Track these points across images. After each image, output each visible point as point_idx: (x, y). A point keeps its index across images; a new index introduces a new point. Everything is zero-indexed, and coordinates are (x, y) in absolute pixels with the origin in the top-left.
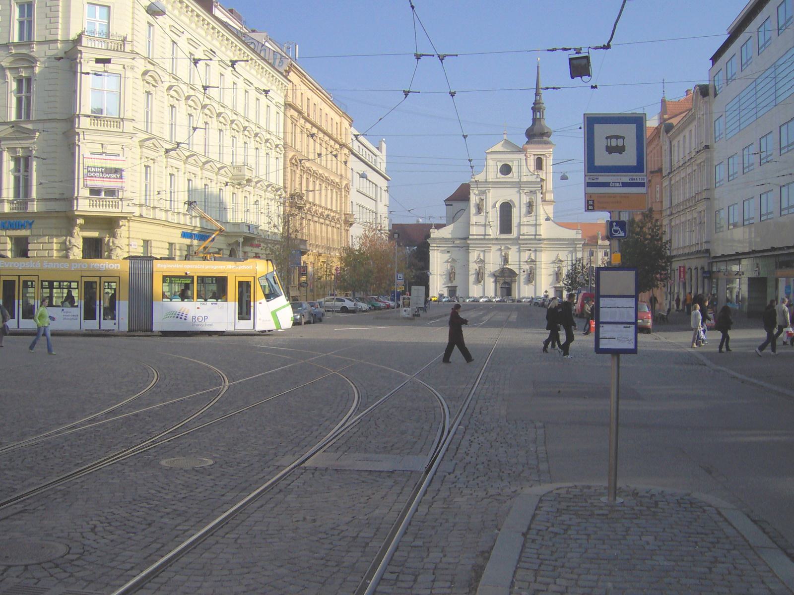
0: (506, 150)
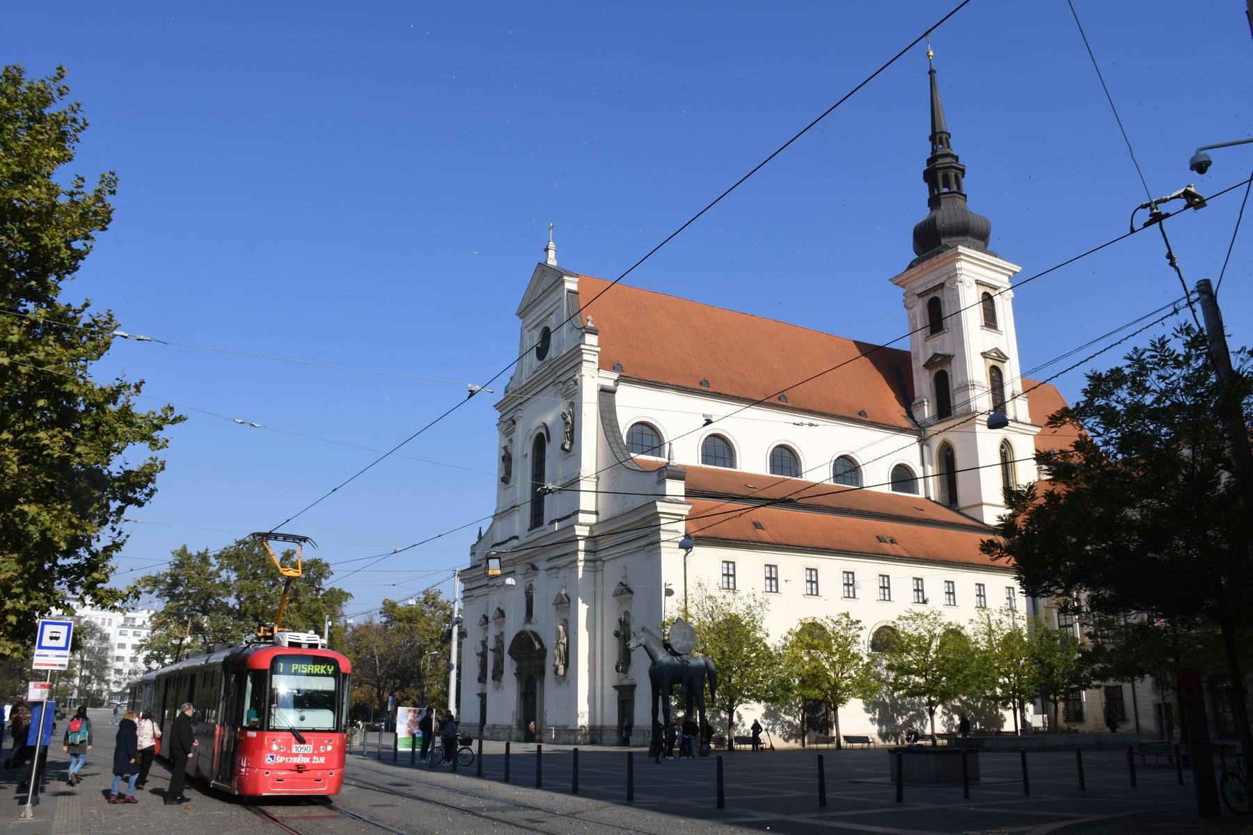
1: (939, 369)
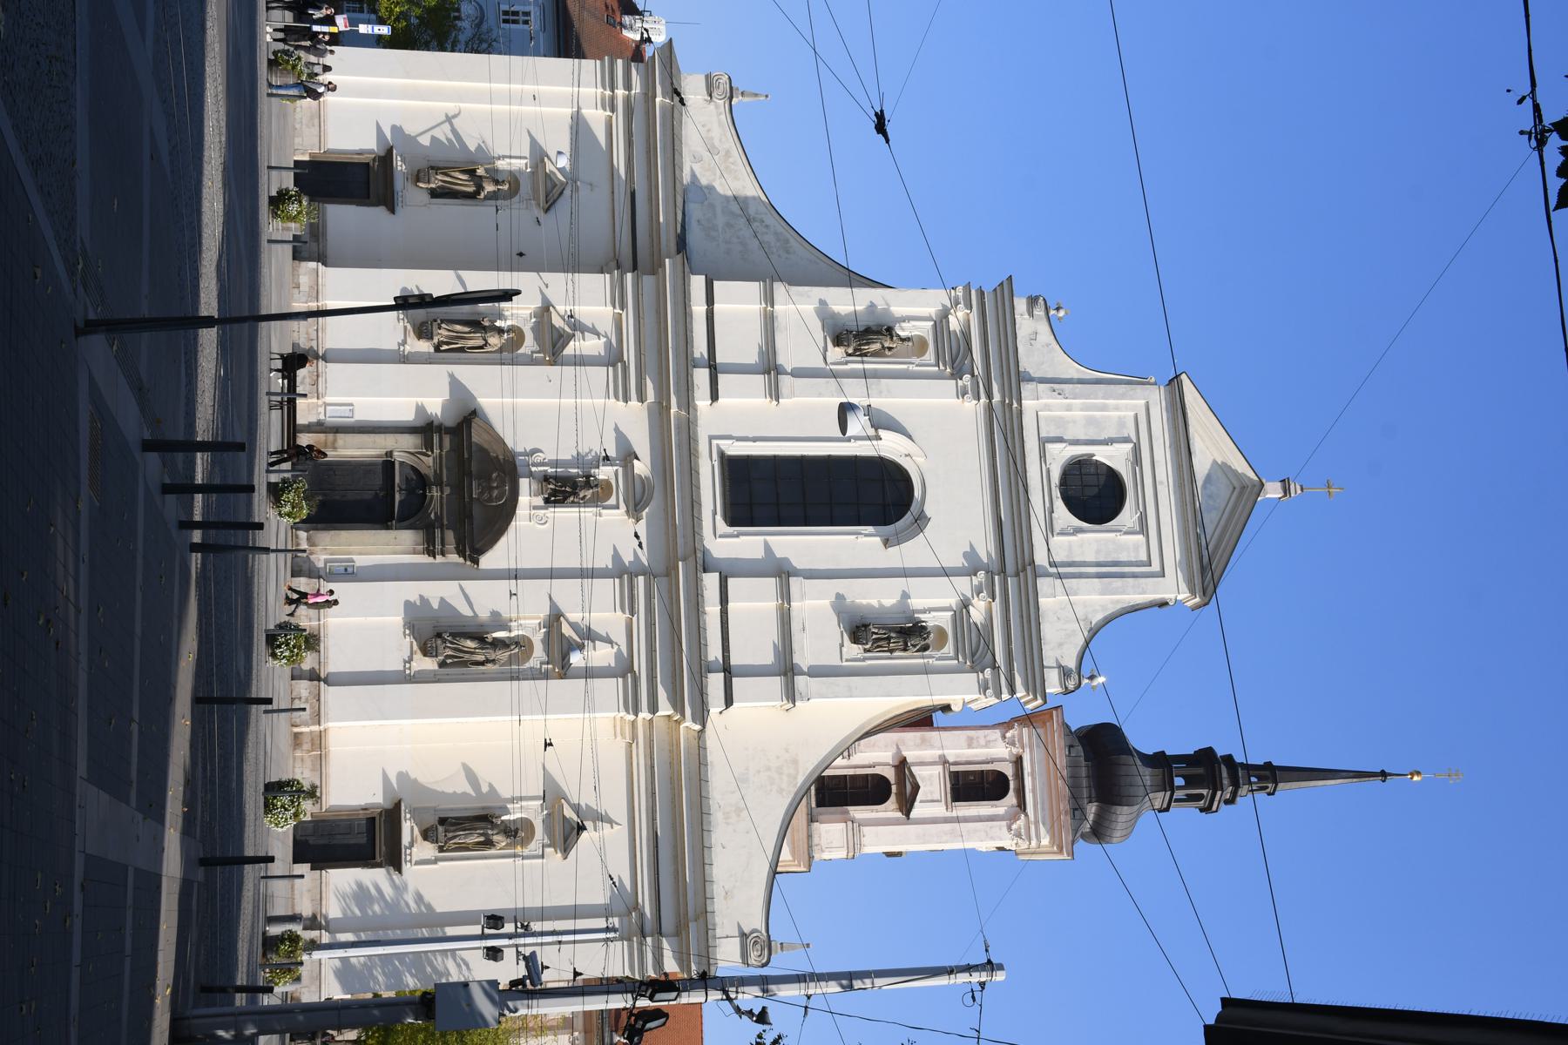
0: (1200, 483)
1: (894, 788)
